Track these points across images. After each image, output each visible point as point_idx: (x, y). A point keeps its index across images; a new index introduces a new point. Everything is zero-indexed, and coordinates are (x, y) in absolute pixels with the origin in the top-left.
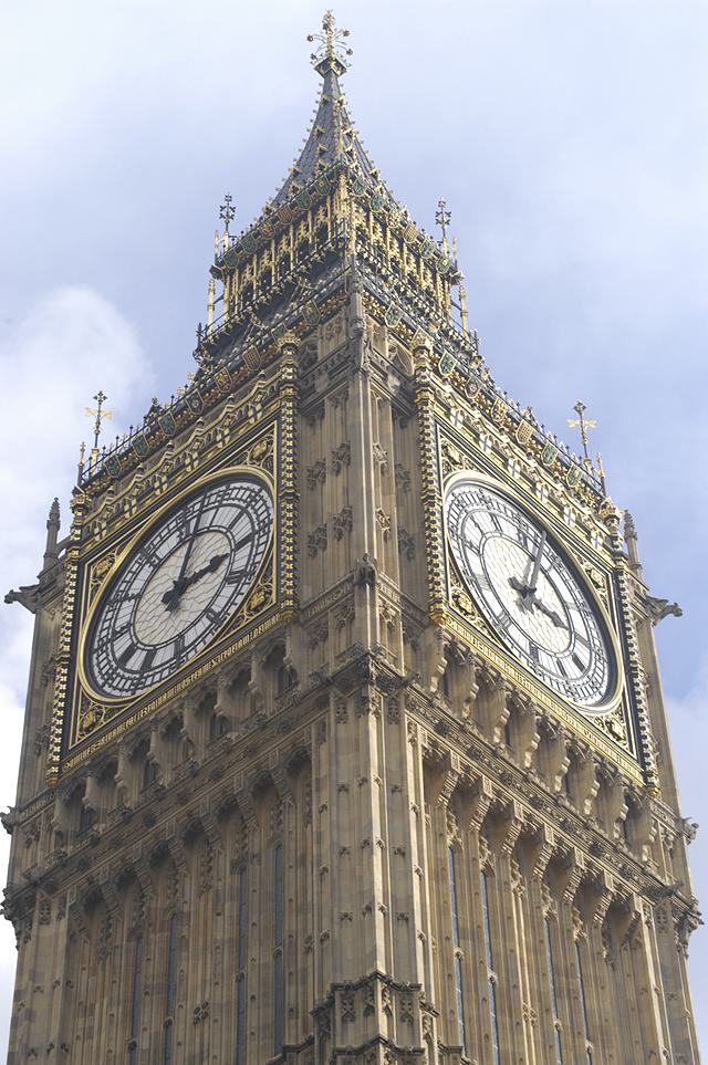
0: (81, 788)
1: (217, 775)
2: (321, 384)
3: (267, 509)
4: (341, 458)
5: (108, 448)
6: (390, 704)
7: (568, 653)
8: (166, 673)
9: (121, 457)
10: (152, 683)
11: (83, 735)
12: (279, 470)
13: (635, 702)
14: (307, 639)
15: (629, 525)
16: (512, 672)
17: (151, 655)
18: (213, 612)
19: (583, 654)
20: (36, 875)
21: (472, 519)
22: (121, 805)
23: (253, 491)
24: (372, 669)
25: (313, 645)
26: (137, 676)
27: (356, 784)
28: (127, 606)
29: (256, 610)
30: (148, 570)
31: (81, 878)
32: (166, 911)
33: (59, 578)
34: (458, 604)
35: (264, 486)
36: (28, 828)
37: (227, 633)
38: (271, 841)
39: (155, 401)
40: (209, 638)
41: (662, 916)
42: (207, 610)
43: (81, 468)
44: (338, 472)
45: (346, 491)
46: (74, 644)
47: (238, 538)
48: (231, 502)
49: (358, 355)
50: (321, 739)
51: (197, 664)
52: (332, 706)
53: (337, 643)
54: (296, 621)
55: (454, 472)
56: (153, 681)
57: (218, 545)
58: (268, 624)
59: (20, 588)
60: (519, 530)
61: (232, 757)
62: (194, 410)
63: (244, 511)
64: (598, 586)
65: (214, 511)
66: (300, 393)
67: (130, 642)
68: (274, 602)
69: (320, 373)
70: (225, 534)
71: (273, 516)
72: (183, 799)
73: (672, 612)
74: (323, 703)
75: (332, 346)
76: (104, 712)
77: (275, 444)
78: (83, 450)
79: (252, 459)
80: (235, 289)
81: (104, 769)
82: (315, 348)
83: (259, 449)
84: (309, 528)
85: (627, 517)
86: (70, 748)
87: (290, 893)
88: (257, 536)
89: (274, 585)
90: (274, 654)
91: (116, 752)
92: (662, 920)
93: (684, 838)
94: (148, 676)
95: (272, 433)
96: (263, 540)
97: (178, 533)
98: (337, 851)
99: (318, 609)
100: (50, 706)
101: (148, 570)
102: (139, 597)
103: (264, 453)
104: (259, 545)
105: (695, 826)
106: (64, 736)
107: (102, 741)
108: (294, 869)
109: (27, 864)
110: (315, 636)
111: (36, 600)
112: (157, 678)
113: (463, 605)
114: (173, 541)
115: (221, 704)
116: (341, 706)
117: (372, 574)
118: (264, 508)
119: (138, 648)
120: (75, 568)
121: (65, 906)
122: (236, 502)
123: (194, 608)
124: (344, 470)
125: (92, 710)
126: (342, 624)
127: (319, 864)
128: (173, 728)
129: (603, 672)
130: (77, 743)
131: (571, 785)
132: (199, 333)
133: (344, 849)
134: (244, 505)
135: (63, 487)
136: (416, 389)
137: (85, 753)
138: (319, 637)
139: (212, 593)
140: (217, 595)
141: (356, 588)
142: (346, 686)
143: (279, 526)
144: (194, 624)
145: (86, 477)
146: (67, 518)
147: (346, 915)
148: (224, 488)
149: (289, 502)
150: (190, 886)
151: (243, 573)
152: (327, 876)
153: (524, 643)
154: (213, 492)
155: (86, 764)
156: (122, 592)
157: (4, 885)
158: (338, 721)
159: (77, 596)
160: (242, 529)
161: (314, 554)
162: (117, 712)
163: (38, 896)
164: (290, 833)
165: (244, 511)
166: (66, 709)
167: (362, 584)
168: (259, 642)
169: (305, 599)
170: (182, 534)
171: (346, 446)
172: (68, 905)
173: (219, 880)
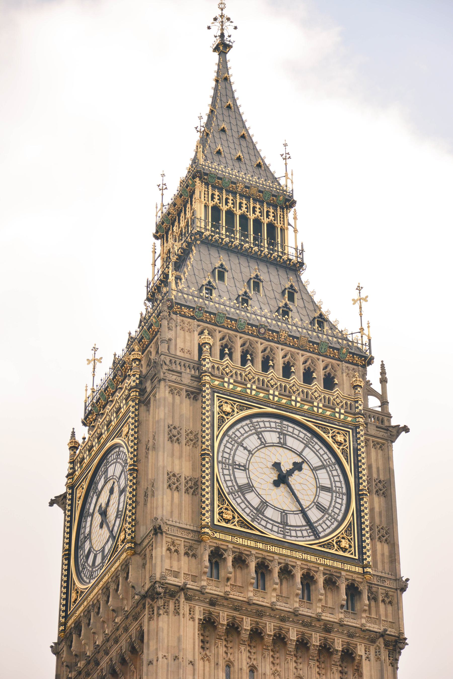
1: (116, 641)
2: (148, 385)
6: (175, 603)
13: (360, 517)
14: (141, 562)
15: (383, 373)
16: (260, 545)
19: (325, 499)
24: (160, 590)
28: (89, 519)
34: (222, 517)
37: (115, 554)
39: (115, 355)
43: (86, 403)
54: (135, 554)
59: (55, 497)
60: (279, 432)
61: (119, 632)
64: (340, 444)
67: (89, 546)
72: (107, 653)
73: (403, 431)
74: (144, 607)
78: (86, 390)
86: (69, 613)
92: (378, 653)
93: (399, 591)
97: (104, 476)
99: (145, 544)
102: (92, 515)
105: (407, 580)
116: (151, 610)
117: (160, 528)
122: (121, 461)
125: (76, 590)
129: (341, 505)
130: (72, 609)
132: (147, 287)
136: (200, 375)
148: (117, 449)
167: (156, 534)
169: (142, 536)
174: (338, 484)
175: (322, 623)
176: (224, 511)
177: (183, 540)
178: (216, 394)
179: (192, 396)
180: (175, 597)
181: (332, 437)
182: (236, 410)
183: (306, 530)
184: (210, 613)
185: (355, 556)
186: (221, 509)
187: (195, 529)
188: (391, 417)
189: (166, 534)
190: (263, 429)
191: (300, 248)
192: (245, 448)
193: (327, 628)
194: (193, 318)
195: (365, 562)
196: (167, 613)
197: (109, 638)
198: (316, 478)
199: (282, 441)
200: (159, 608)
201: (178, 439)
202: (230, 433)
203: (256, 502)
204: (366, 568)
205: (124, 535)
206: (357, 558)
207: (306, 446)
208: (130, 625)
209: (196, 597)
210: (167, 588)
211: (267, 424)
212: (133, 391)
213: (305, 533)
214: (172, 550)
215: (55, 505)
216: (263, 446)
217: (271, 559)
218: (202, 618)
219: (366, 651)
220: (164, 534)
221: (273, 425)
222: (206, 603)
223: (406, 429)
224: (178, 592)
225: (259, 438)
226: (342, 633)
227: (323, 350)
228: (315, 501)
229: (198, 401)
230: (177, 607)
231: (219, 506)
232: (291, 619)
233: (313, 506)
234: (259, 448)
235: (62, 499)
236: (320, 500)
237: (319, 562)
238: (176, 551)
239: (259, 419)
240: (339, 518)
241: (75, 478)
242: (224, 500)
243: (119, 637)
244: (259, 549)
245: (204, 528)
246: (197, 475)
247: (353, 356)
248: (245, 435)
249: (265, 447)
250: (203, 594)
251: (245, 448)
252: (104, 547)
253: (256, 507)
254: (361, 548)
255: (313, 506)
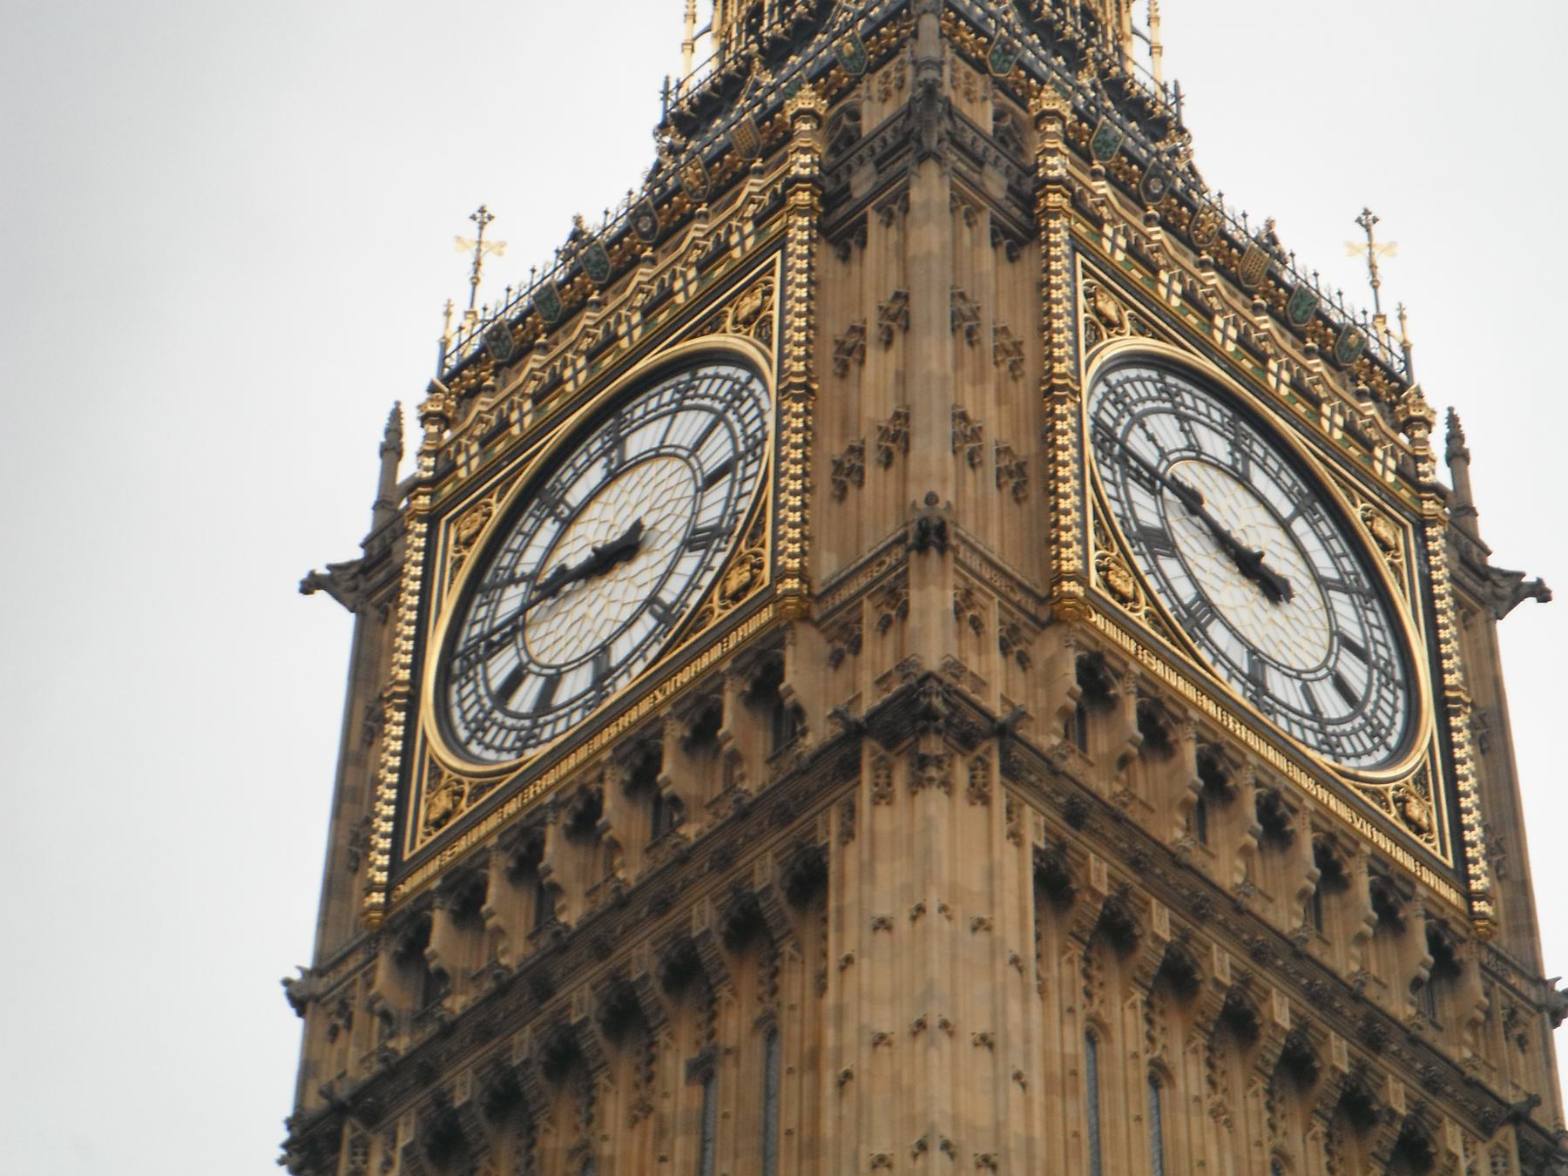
0: (424, 931)
1: (662, 906)
2: (862, 182)
3: (761, 414)
4: (894, 318)
5: (491, 308)
6: (972, 769)
7: (1324, 672)
8: (576, 717)
9: (513, 325)
10: (554, 736)
11: (429, 834)
12: (782, 342)
13: (1450, 763)
14: (826, 650)
16: (1210, 707)
17: (552, 684)
18: (661, 603)
19: (1355, 672)
20: (343, 1092)
21: (1143, 426)
22: (495, 963)
23: (736, 381)
24: (937, 702)
25: (837, 660)
26: (527, 723)
27: (906, 915)
29: (736, 597)
30: (549, 529)
31: (422, 1097)
32: (572, 1154)
33: (397, 547)
35: (756, 372)
36: (333, 1006)
38: (758, 1023)
40: (652, 653)
41: (1500, 1160)
42: (652, 600)
43: (444, 344)
44: (888, 343)
45: (902, 379)
46: (417, 667)
47: (710, 467)
48: (696, 401)
49: (928, 126)
50: (848, 835)
51: (631, 699)
52: (866, 774)
53: (877, 655)
54: (805, 617)
55: (1106, 341)
56: (556, 730)
57: (673, 481)
58: (753, 625)
59: (329, 567)
60: (1232, 443)
61: (689, 871)
62: (644, 236)
63: (720, 418)
64: (1385, 547)
65: (667, 420)
66: (824, 200)
68: (767, 583)
69: (861, 161)
70: (686, 460)
71: (771, 427)
74: (850, 769)
75: (889, 110)
76: (467, 789)
77: (776, 296)
78: (448, 314)
79: (735, 322)
80: (733, 12)
81: (464, 892)
82: (855, 116)
83: (749, 304)
84: (833, 447)
85: (1453, 421)
86: (407, 855)
87: (789, 1118)
88: (741, 463)
89: (767, 552)
90: (763, 675)
91: (486, 865)
93: (1547, 1016)
94: (546, 723)
95: (772, 274)
96: (751, 470)
97: (604, 460)
98: (868, 1038)
99: (846, 593)
100: (377, 782)
101: (549, 529)
103: (757, 312)
104: (744, 480)
106: (397, 836)
107: (462, 845)
108: (797, 1073)
109: (328, 1073)
110: (839, 645)
111: (356, 588)
112: (561, 726)
113: (1118, 582)
114: (596, 474)
115: (672, 771)
117: (941, 530)
118: (755, 412)
119: (530, 672)
120: (423, 528)
121: (394, 1147)
122: (707, 402)
123: (630, 598)
124: (898, 339)
125: (446, 787)
126: (885, 624)
127: (838, 1061)
128: (585, 820)
129: (1394, 706)
130: (419, 847)
131: (1324, 916)
132: (666, 94)
133: (882, 1037)
134: (719, 406)
135: (412, 380)
136: (1036, 190)
137: (433, 866)
138: (845, 644)
139: (661, 569)
140: (669, 572)
141: (913, 555)
142: (891, 740)
143: (779, 443)
144: (627, 626)
145: (452, 362)
146: (414, 436)
147: (882, 1159)
148: (685, 377)
149: (797, 399)
150: (614, 1107)
151: (716, 532)
152: (851, 1086)
153: (1239, 656)
154: (667, 384)
155: (436, 884)
156: (505, 569)
157: (288, 1110)
158: (882, 797)
159: (426, 579)
160: (718, 450)
161: (841, 494)
162: (489, 789)
163: (347, 1131)
164: (792, 1008)
165: (720, 418)
166: (402, 787)
167: (922, 547)
168: (740, 657)
170: (611, 461)
171: (902, 297)
172: (401, 1144)
173: (666, 1095)
174: (1382, 651)
175: (1362, 1010)
176: (1113, 565)
177: (997, 599)
178: (1079, 257)
179: (1005, 243)
180: (972, 747)
181: (1365, 520)
182: (1128, 325)
183: (1311, 729)
184: (1061, 847)
185: (1444, 853)
186: (1102, 557)
187: (1027, 583)
188: (1489, 553)
189: (957, 560)
190: (1190, 412)
191: (1171, 89)
192: (1151, 438)
193: (1374, 1032)
194: (979, 65)
195: (1476, 885)
196: (947, 785)
197: (629, 896)
198: (1329, 610)
199: (1240, 467)
200: (922, 762)
201: (970, 333)
202: (1114, 378)
203: (1186, 592)
204: (1479, 900)
205: (747, 574)
206: (1450, 863)
207: (1299, 512)
208: (750, 839)
209: (1030, 773)
210: (955, 708)
211: (1202, 407)
212: (804, 190)
213: (1311, 740)
214: (965, 611)
215: (321, 595)
216: (1193, 454)
217: (1238, 759)
218: (1042, 845)
219: (1466, 1150)
220: (950, 555)
221: (1216, 415)
222: (1057, 807)
223: (1541, 593)
224: (986, 737)
225: (1182, 429)
226: (1408, 1068)
227: (1299, 313)
228: (1331, 664)
229: (1017, 264)
230: (979, 781)
231: (1097, 549)
232: (1280, 963)
233: (1324, 677)
234: (1186, 454)
235: (354, 577)
236: (1341, 668)
237: (1358, 826)
238: (976, 624)
239: (1182, 384)
240: (1393, 741)
241: (448, 489)
242: (1107, 539)
243: (683, 888)
244: (1206, 713)
245: (1069, 580)
246: (1026, 447)
247: (1372, 365)
248: (1149, 405)
249: (1197, 459)
250: (1056, 773)
251: (1151, 438)
252: (605, 648)
253: (1186, 601)
254: (1460, 845)
255: (1324, 677)
